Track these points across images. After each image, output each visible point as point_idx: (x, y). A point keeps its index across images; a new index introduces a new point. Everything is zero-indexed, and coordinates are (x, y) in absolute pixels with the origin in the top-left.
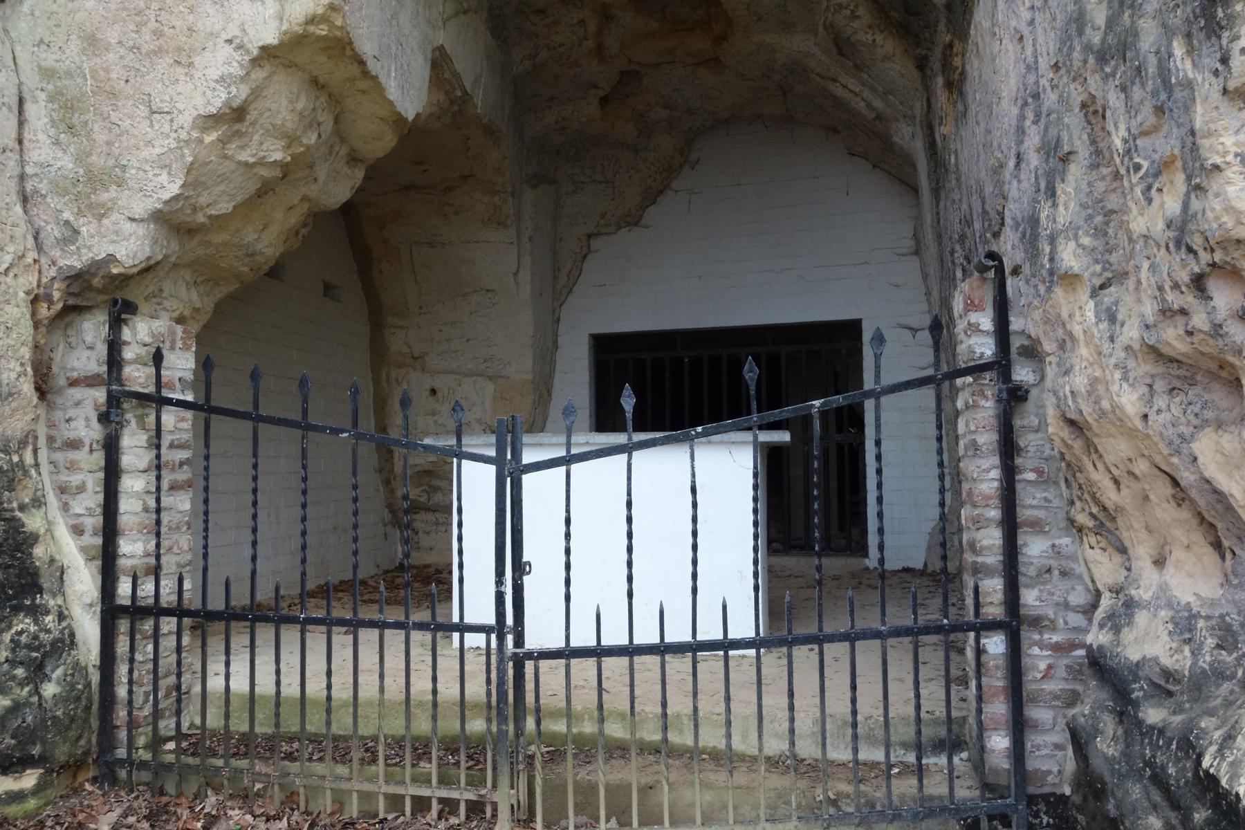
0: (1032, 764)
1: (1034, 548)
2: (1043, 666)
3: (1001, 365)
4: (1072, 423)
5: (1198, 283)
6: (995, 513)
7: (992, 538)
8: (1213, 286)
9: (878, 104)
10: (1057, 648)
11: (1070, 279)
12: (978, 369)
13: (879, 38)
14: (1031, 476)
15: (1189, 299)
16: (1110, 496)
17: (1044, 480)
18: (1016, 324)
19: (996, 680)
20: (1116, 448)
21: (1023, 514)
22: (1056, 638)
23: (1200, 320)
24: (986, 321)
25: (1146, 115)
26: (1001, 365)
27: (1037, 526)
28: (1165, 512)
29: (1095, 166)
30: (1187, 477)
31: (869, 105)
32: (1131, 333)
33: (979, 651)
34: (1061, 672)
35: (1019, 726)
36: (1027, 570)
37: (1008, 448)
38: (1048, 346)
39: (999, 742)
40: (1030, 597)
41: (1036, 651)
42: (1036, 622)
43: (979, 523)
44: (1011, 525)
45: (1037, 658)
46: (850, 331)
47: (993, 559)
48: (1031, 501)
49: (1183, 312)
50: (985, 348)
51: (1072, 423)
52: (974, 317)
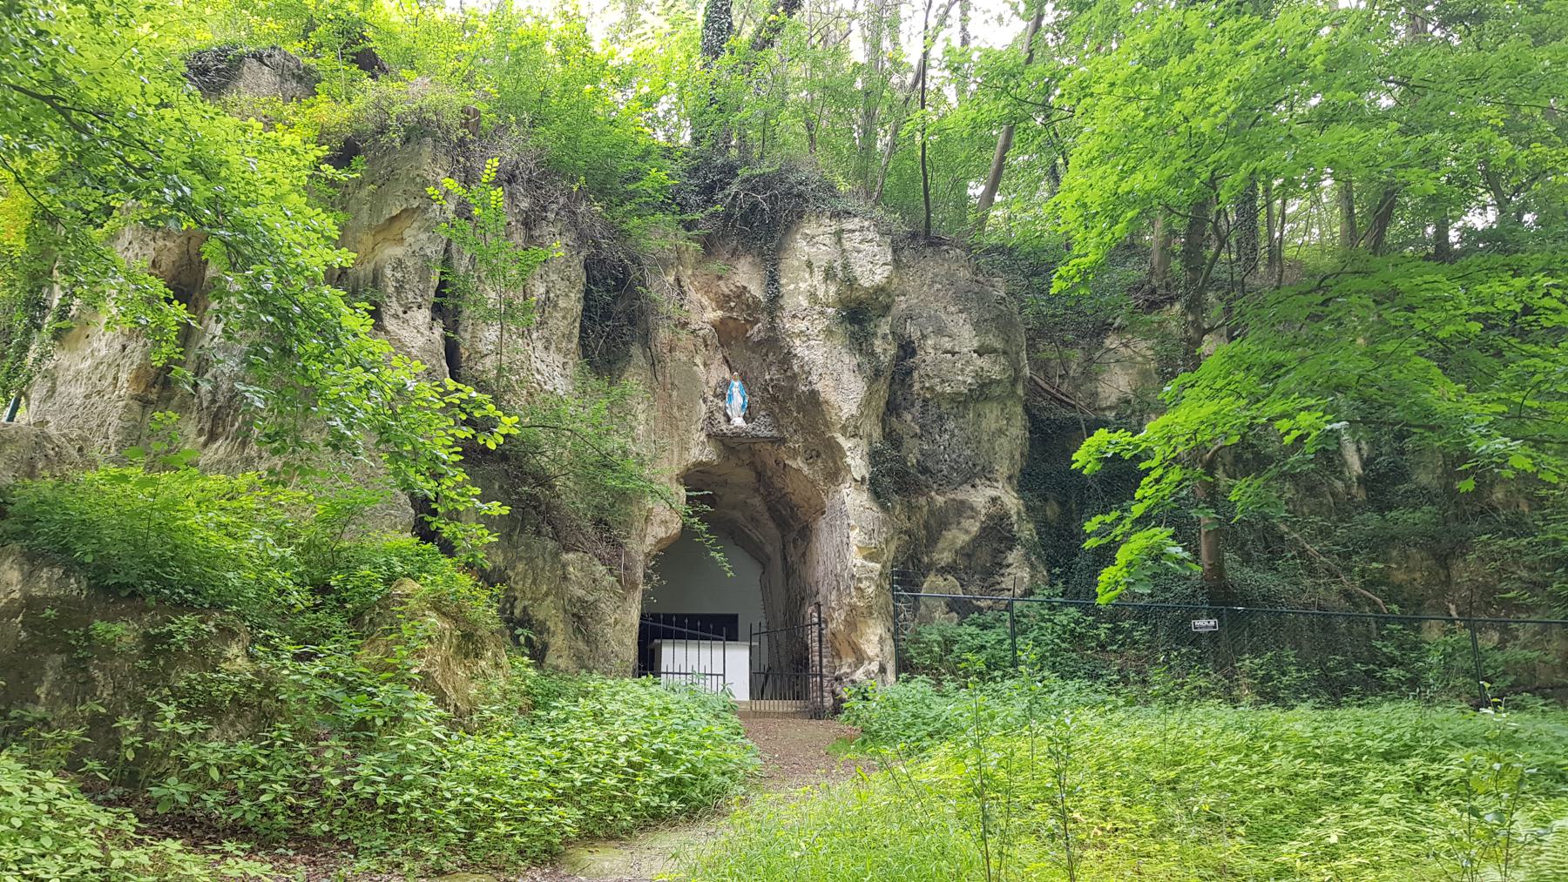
1: (825, 660)
20: (840, 637)
37: (820, 641)
45: (825, 684)
50: (816, 620)
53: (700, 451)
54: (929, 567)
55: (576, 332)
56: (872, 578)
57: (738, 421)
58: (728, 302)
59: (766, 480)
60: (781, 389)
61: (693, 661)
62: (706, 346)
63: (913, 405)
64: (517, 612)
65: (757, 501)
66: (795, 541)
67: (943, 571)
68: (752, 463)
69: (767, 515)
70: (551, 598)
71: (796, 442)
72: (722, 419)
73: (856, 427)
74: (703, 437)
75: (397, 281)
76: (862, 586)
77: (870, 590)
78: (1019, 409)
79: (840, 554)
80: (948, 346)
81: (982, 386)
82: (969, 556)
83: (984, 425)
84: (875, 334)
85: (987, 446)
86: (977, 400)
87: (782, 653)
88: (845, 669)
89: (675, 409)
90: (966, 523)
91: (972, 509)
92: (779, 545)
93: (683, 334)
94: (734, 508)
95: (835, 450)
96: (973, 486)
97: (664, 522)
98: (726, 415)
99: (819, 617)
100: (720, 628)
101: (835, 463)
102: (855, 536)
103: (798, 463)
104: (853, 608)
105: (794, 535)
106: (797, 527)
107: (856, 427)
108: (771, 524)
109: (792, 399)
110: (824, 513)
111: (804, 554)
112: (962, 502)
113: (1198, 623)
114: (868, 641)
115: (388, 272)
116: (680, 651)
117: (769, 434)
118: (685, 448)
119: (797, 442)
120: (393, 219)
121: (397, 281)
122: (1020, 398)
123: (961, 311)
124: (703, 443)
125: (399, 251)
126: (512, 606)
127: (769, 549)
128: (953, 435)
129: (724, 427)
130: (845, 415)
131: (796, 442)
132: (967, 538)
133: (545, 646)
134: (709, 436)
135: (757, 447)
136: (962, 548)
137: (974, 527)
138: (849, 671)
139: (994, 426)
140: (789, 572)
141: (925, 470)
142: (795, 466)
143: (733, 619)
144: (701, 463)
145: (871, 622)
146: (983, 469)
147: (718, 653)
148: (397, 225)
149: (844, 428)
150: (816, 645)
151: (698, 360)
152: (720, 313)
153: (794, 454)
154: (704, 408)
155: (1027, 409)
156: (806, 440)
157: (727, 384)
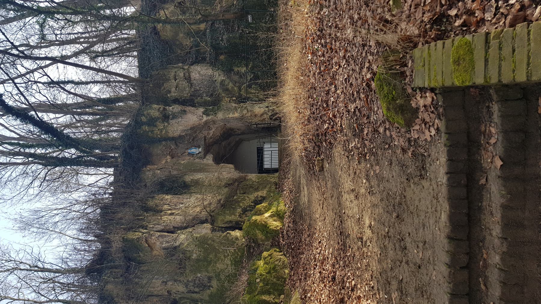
3: (256, 125)
26: (256, 125)
37: (261, 124)
46: (257, 148)
48: (264, 123)
53: (209, 160)
54: (240, 94)
55: (177, 196)
57: (200, 150)
59: (216, 142)
60: (190, 138)
61: (268, 159)
63: (193, 99)
64: (252, 204)
65: (223, 143)
66: (234, 132)
67: (240, 90)
68: (212, 145)
70: (249, 196)
71: (205, 133)
72: (200, 154)
75: (166, 243)
78: (192, 67)
79: (237, 119)
80: (174, 89)
81: (186, 79)
82: (236, 83)
83: (198, 78)
84: (172, 112)
85: (203, 77)
86: (190, 80)
87: (266, 134)
90: (226, 83)
91: (222, 81)
95: (206, 123)
96: (216, 81)
98: (198, 153)
100: (260, 152)
101: (211, 122)
102: (231, 115)
103: (211, 132)
104: (251, 115)
107: (200, 116)
112: (220, 84)
113: (250, 20)
114: (260, 111)
115: (164, 245)
116: (265, 163)
117: (203, 141)
118: (208, 165)
120: (149, 246)
121: (166, 243)
122: (189, 67)
123: (163, 85)
125: (158, 243)
126: (251, 206)
127: (237, 139)
128: (201, 87)
131: (205, 133)
132: (231, 83)
133: (261, 196)
134: (204, 158)
135: (207, 144)
136: (233, 84)
137: (228, 81)
139: (198, 75)
140: (243, 133)
141: (212, 95)
143: (257, 148)
144: (213, 160)
146: (210, 78)
147: (265, 153)
148: (150, 244)
149: (200, 120)
150: (263, 125)
151: (183, 162)
152: (168, 157)
153: (208, 134)
155: (192, 65)
156: (205, 130)
157: (189, 154)
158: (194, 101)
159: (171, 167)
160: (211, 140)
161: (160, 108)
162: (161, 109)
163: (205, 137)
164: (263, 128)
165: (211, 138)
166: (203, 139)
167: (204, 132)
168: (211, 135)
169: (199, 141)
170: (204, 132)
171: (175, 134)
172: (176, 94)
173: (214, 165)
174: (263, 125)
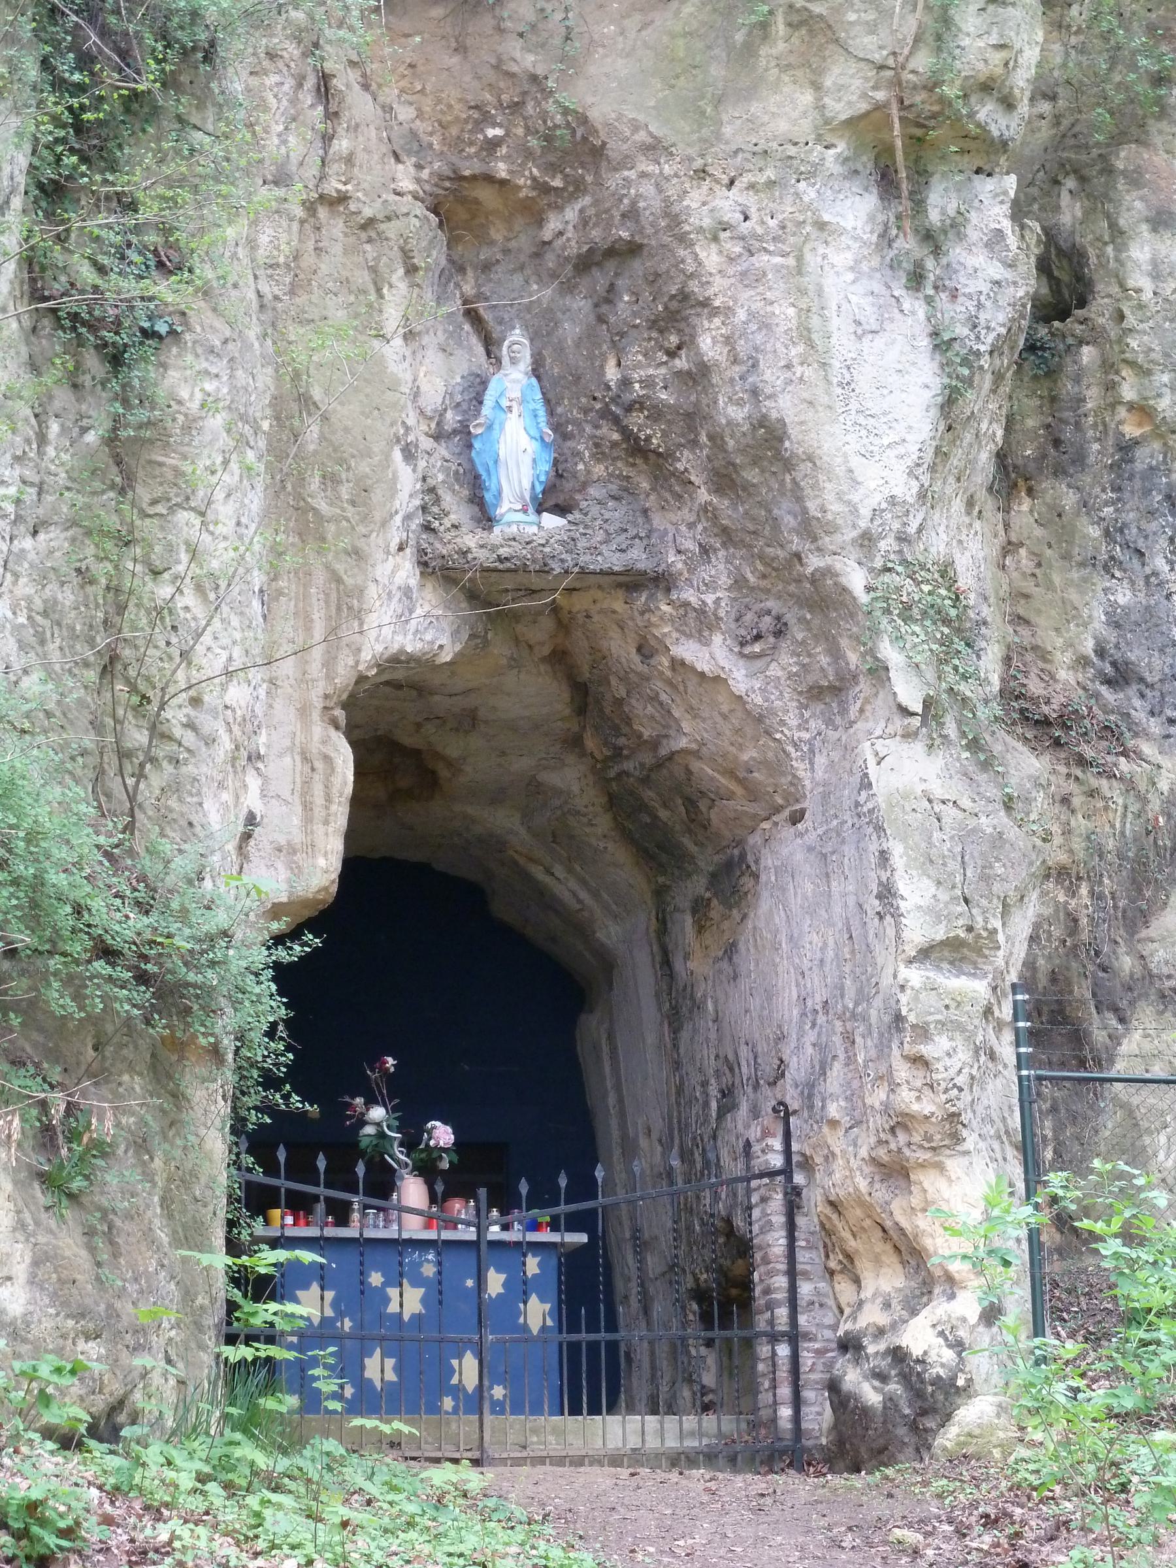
0: (804, 1425)
1: (805, 1289)
2: (810, 1363)
3: (787, 1172)
4: (832, 1204)
5: (892, 1130)
6: (783, 1267)
7: (781, 1281)
8: (899, 1132)
9: (583, 895)
10: (820, 1353)
11: (833, 1124)
12: (772, 1174)
13: (611, 846)
14: (803, 1244)
15: (890, 1137)
16: (852, 1244)
17: (810, 1247)
18: (795, 1147)
19: (783, 1373)
21: (799, 1267)
22: (817, 1346)
23: (893, 1146)
24: (777, 1144)
25: (873, 1053)
26: (787, 1172)
27: (806, 1275)
28: (880, 1246)
29: (847, 1065)
30: (888, 1224)
31: (575, 894)
32: (864, 1152)
33: (774, 1354)
34: (820, 1367)
35: (797, 1402)
36: (802, 1303)
38: (818, 1160)
39: (785, 1412)
40: (802, 1320)
41: (805, 1354)
42: (808, 1337)
43: (771, 1274)
44: (792, 1273)
45: (807, 1359)
47: (781, 1296)
48: (802, 1257)
49: (887, 1142)
50: (777, 1161)
51: (832, 1204)
52: (770, 1141)
56: (960, 1027)
58: (479, 126)
62: (411, 270)
66: (699, 907)
68: (559, 658)
69: (604, 823)
73: (902, 538)
74: (406, 571)
76: (926, 1050)
77: (955, 1063)
88: (872, 1316)
89: (315, 483)
92: (644, 920)
93: (335, 228)
94: (497, 797)
97: (287, 851)
99: (787, 1152)
101: (836, 654)
104: (902, 1122)
105: (698, 886)
106: (708, 860)
107: (902, 538)
108: (619, 854)
109: (694, 443)
110: (797, 818)
111: (731, 950)
117: (616, 562)
119: (711, 586)
124: (407, 592)
129: (470, 541)
130: (868, 496)
135: (579, 603)
138: (882, 1319)
142: (703, 666)
144: (397, 660)
145: (954, 1165)
150: (777, 1242)
154: (407, 479)
156: (739, 583)
158: (1059, 471)
159: (333, 186)
160: (621, 649)
161: (1008, 104)
162: (987, 112)
163: (662, 581)
164: (742, 1247)
165: (646, 650)
166: (638, 558)
167: (719, 570)
168: (688, 651)
169: (617, 514)
170: (719, 570)
171: (711, 258)
172: (1140, 280)
173: (344, 676)
174: (777, 1242)
